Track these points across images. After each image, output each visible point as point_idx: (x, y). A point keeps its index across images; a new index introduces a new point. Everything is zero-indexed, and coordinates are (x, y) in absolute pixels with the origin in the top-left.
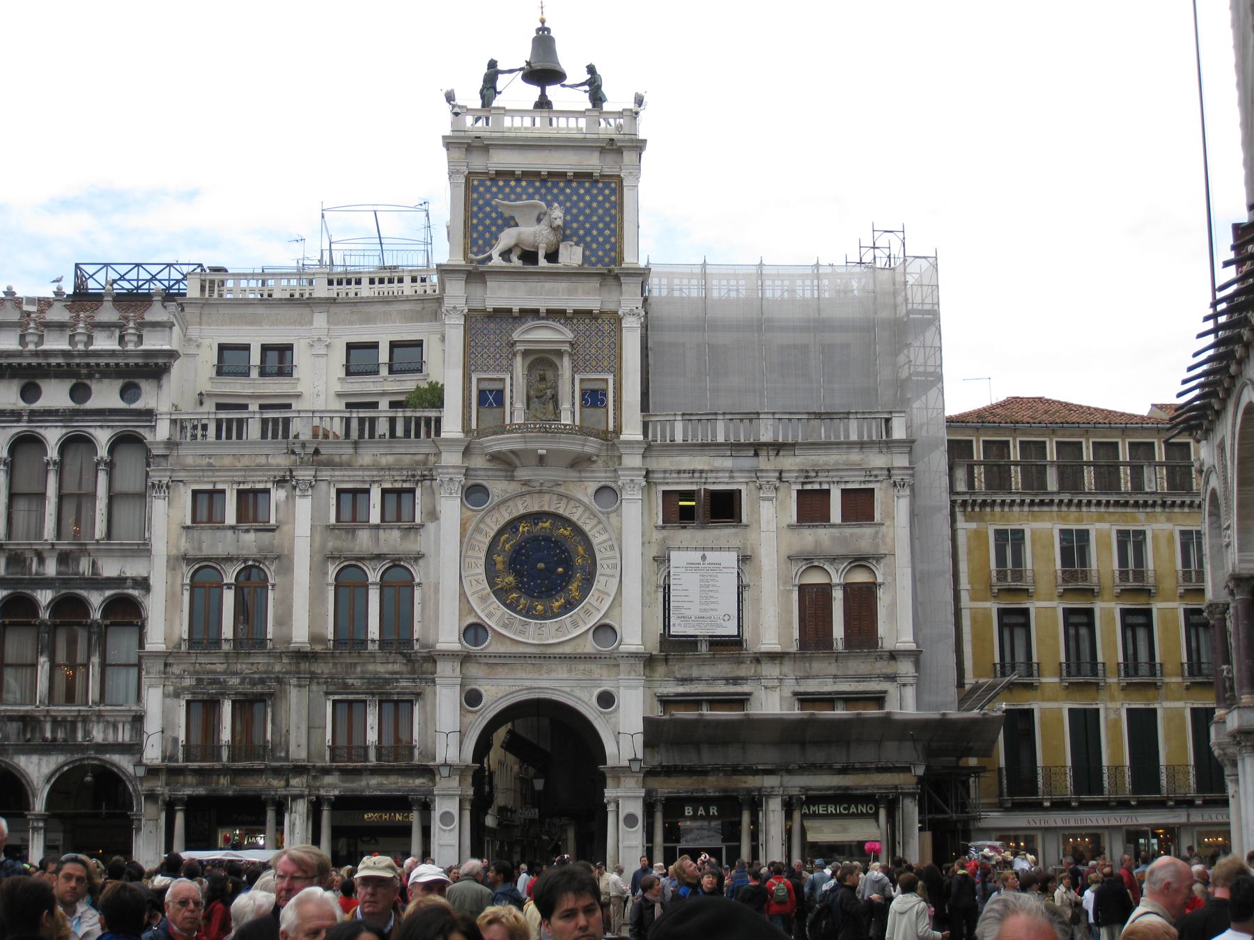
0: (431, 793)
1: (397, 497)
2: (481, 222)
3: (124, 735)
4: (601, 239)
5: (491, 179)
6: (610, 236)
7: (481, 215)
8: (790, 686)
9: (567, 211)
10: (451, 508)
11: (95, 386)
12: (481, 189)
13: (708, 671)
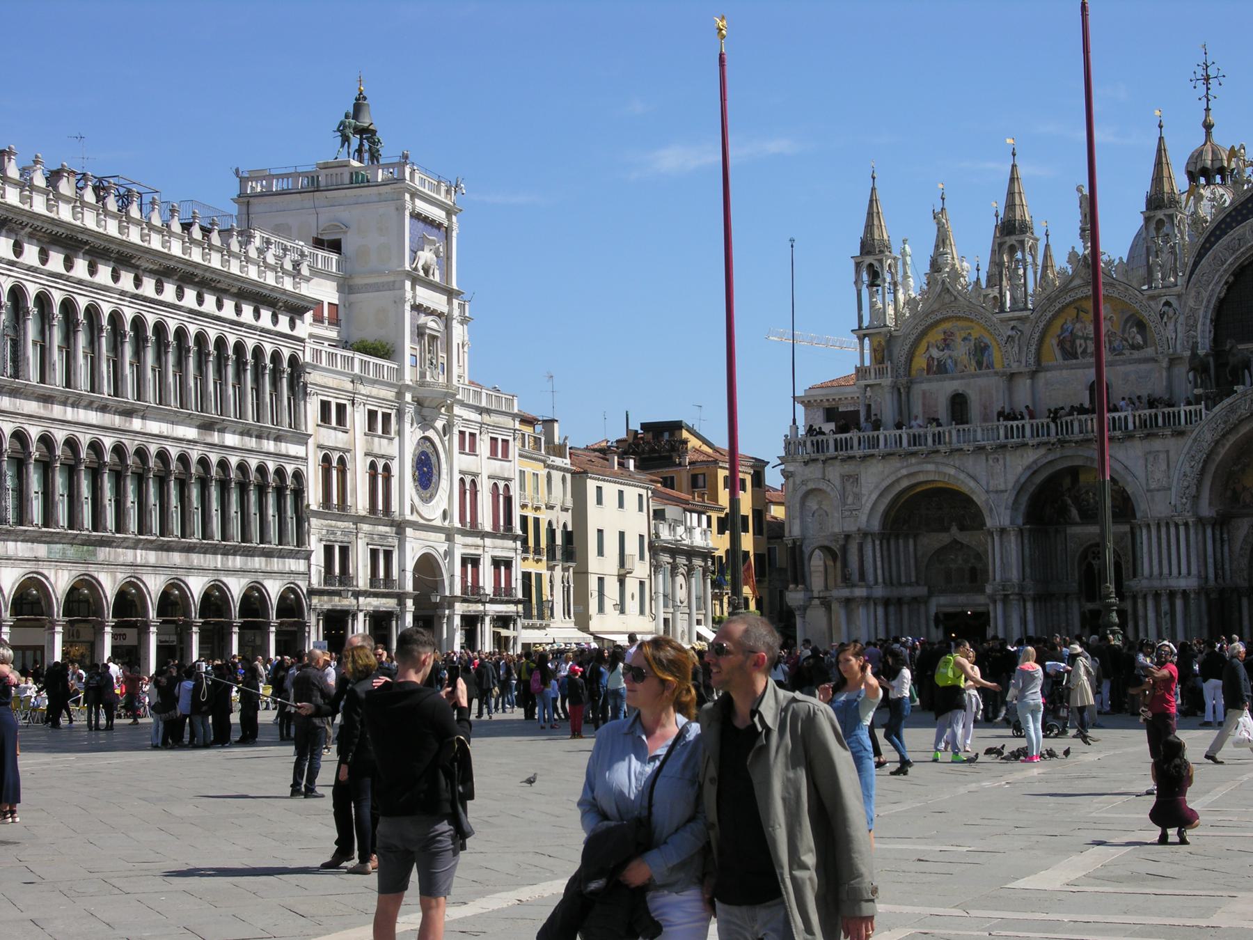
1: (386, 417)
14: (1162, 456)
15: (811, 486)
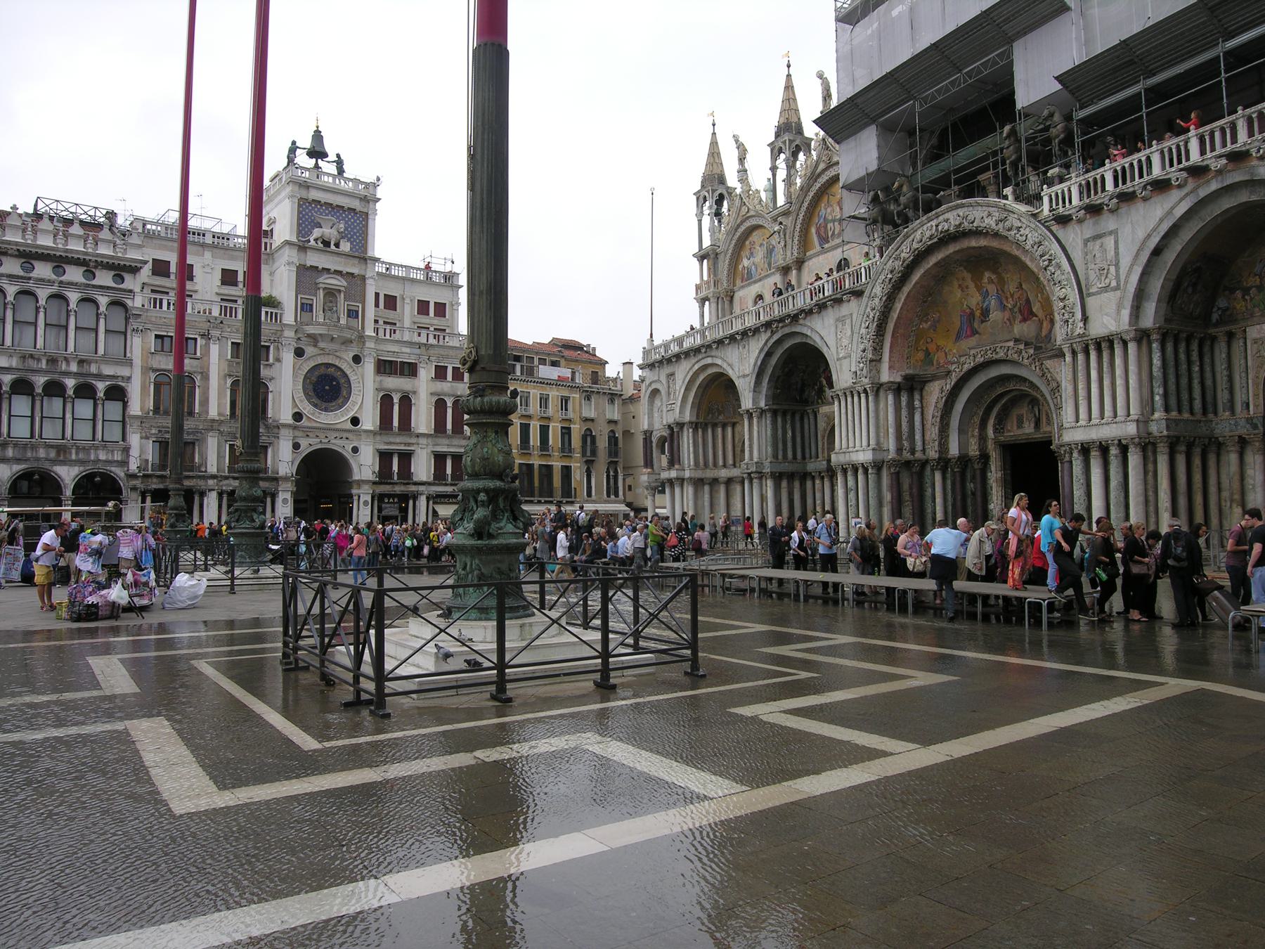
0: (277, 489)
3: (118, 456)
8: (431, 448)
10: (288, 357)
11: (98, 273)
13: (398, 440)
14: (848, 321)
15: (654, 386)
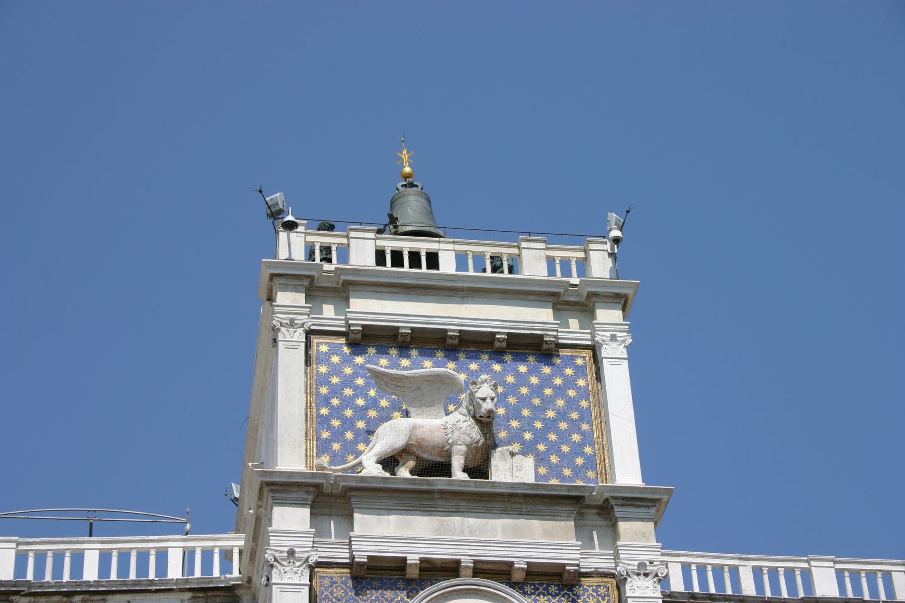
2: (336, 412)
4: (565, 449)
5: (352, 344)
6: (581, 445)
7: (335, 402)
9: (501, 399)
12: (335, 359)
